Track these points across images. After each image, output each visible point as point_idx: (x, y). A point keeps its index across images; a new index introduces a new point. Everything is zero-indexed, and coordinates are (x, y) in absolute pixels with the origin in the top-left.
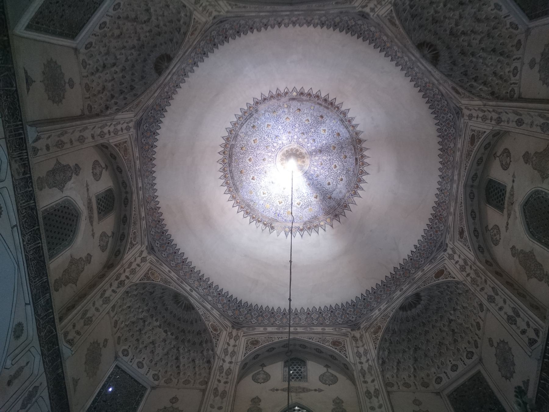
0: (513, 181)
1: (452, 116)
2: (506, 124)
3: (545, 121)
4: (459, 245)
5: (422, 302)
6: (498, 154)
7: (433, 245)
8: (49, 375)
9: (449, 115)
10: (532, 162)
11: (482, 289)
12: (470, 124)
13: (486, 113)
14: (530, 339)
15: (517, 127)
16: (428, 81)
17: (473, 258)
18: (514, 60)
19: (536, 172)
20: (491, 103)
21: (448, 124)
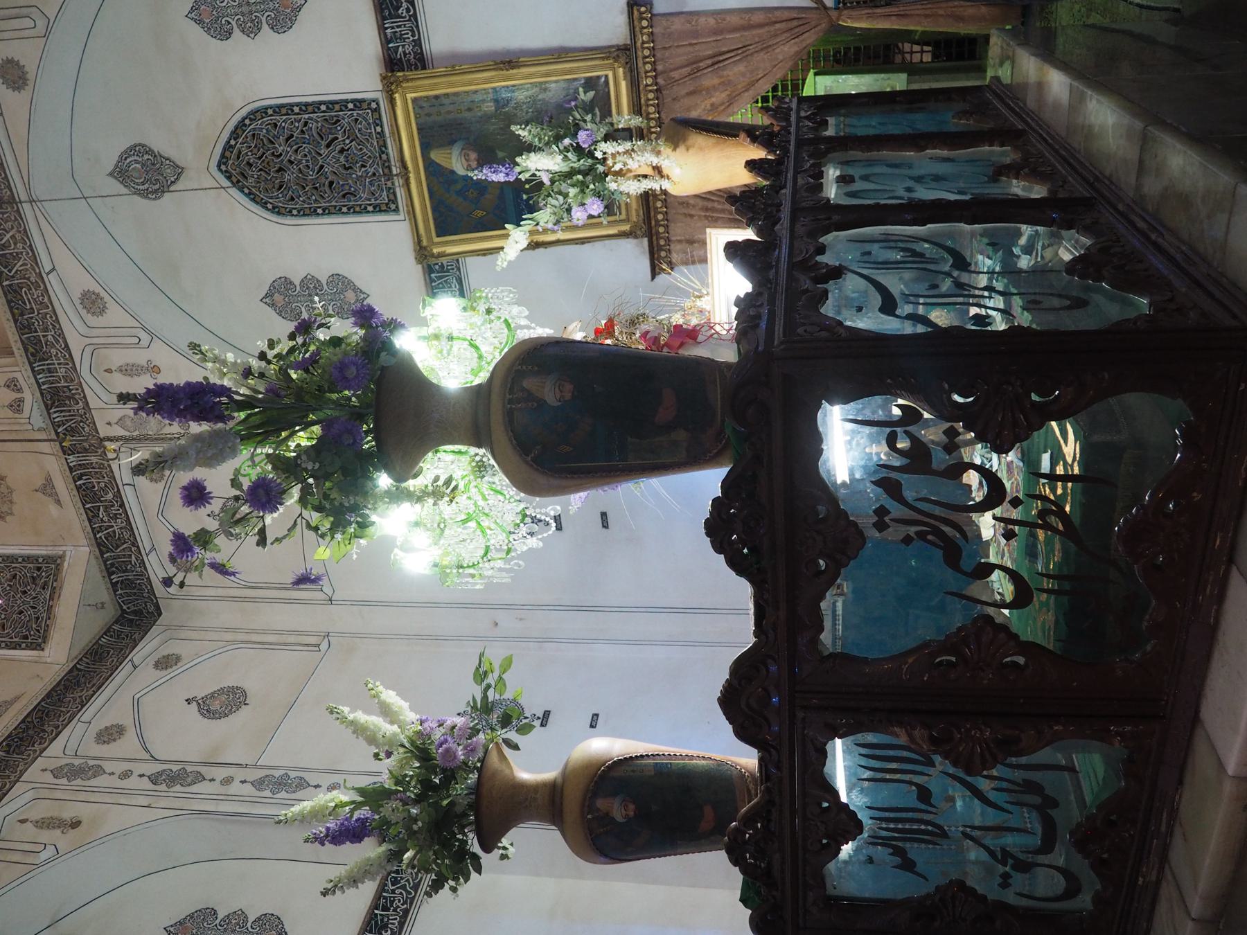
8: (20, 768)
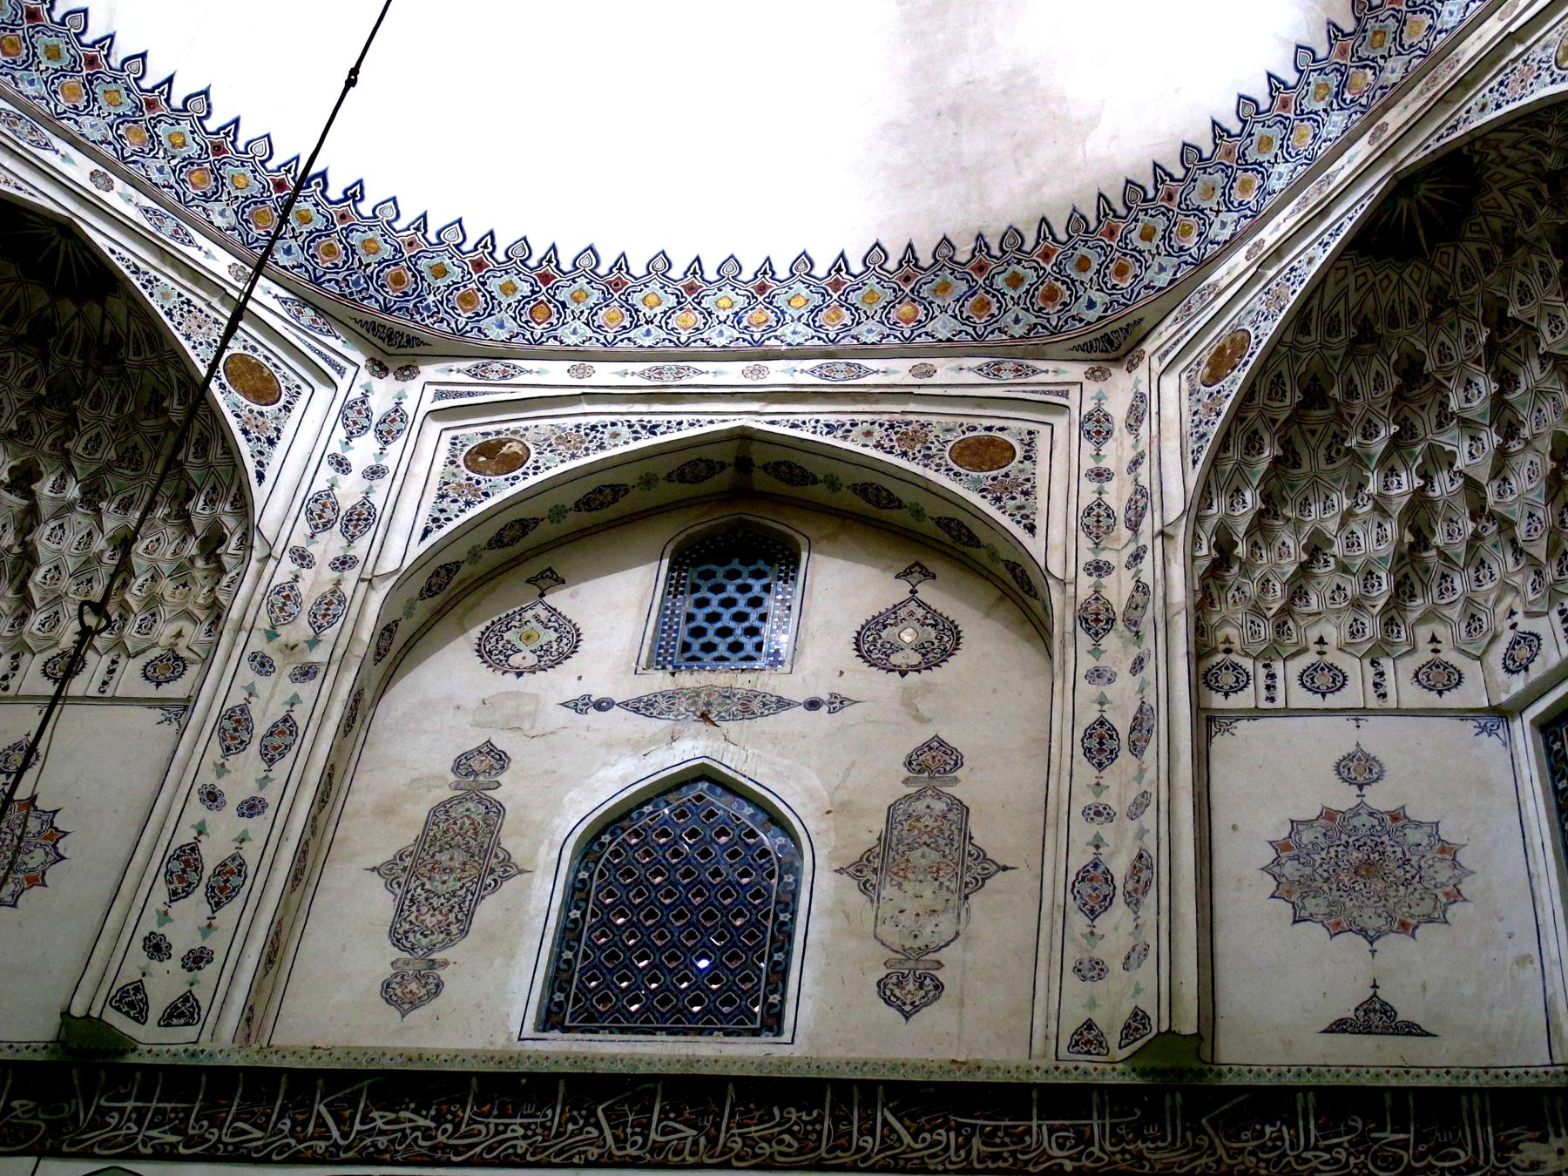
0: (813, 705)
1: (1091, 315)
2: (1087, 663)
3: (1119, 882)
4: (430, 453)
5: (68, 308)
6: (926, 592)
7: (392, 294)
9: (1100, 298)
10: (919, 796)
11: (263, 664)
12: (1060, 422)
13: (1126, 534)
14: (138, 988)
15: (1079, 734)
16: (1276, 184)
17: (390, 562)
18: (1373, 663)
19: (880, 825)
20: (1177, 572)
21: (1051, 295)
